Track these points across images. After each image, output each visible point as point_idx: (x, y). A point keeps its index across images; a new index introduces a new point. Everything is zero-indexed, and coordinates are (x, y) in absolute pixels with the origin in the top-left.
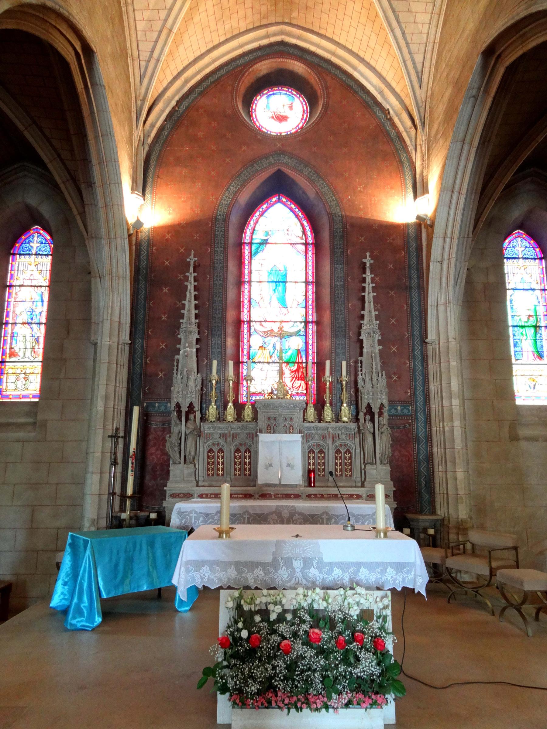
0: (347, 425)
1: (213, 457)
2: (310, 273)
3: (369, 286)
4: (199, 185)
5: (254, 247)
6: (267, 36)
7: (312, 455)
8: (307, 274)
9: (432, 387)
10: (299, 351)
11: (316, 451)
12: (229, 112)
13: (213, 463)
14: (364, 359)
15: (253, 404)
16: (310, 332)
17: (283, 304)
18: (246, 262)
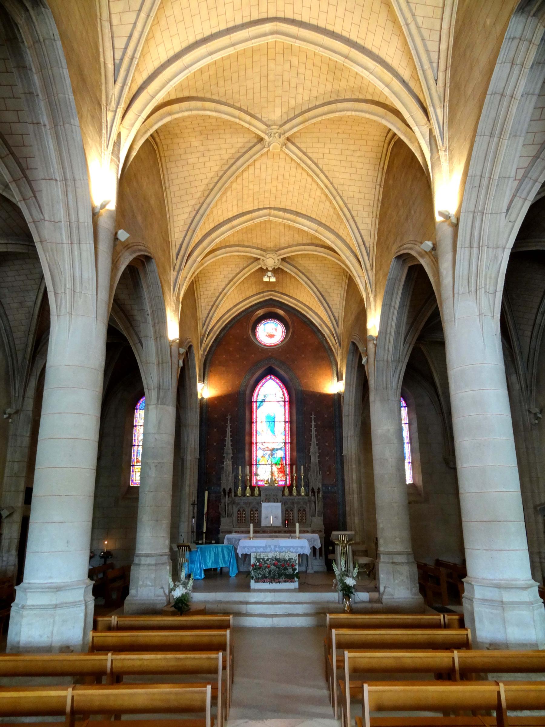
0: (304, 497)
1: (240, 514)
2: (287, 417)
3: (313, 429)
4: (230, 375)
5: (258, 403)
6: (263, 297)
7: (287, 512)
8: (285, 417)
9: (346, 477)
10: (281, 458)
11: (289, 510)
12: (245, 337)
13: (240, 517)
14: (311, 465)
15: (259, 487)
16: (287, 448)
17: (273, 432)
18: (255, 412)
